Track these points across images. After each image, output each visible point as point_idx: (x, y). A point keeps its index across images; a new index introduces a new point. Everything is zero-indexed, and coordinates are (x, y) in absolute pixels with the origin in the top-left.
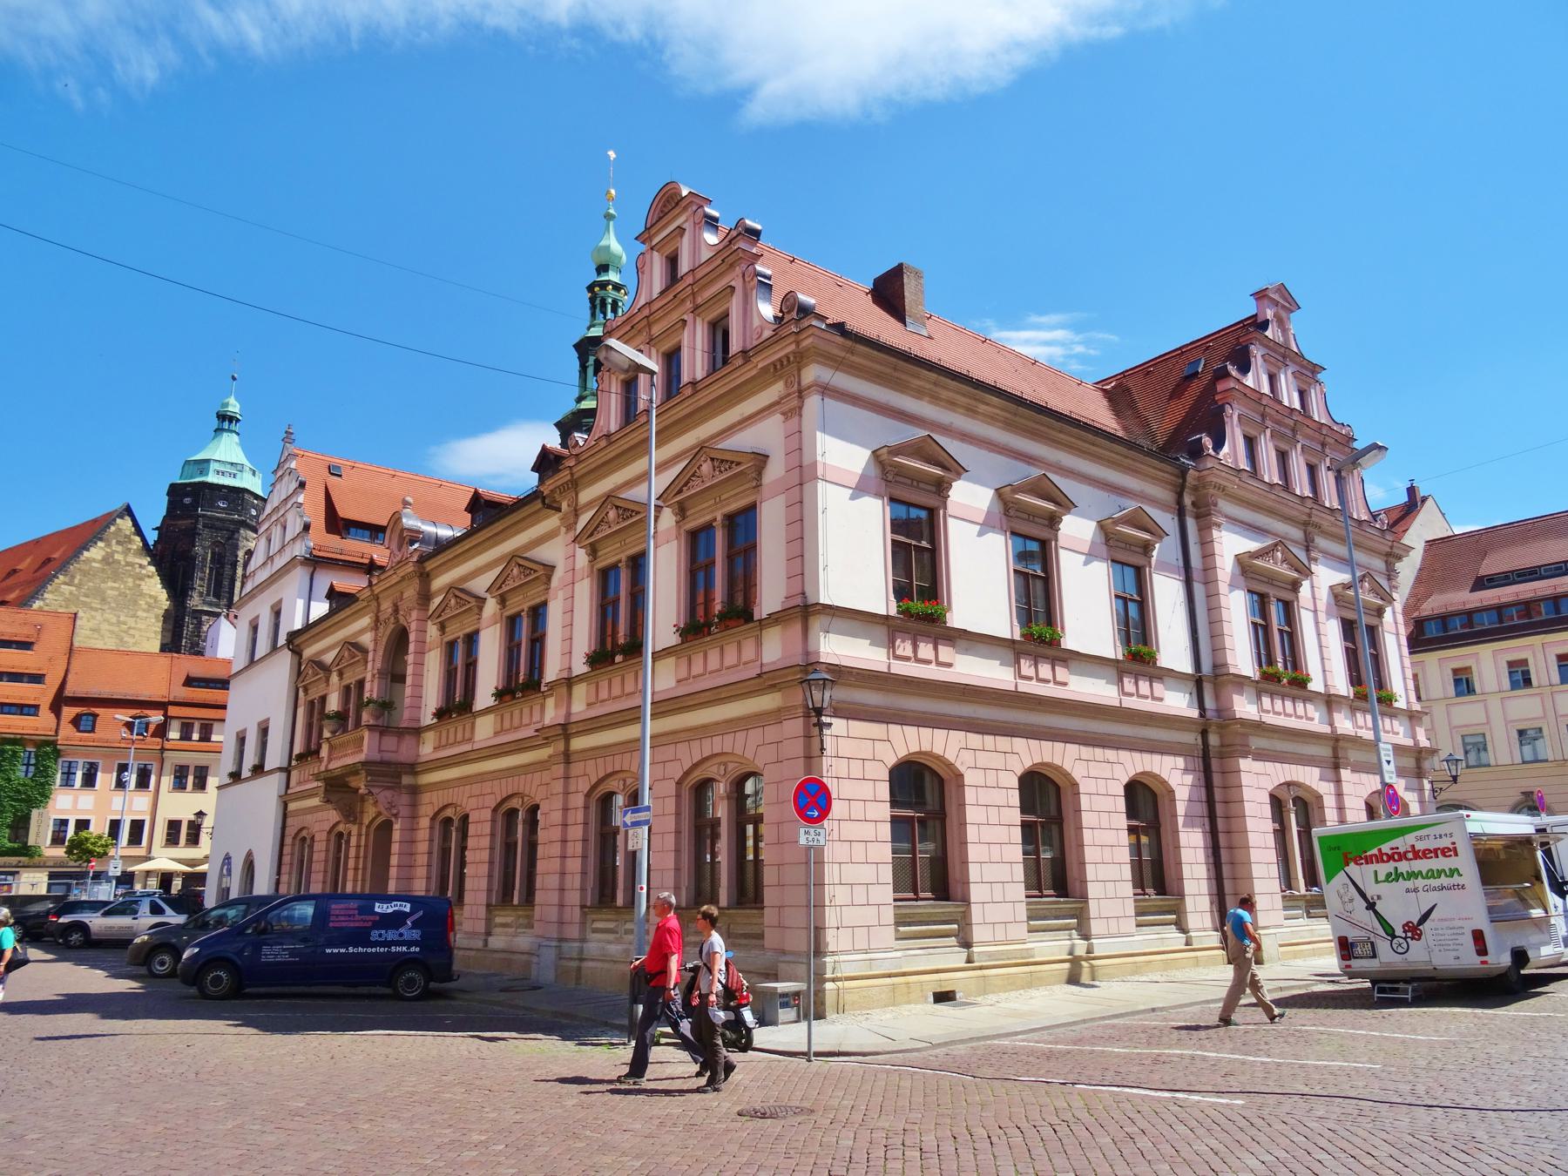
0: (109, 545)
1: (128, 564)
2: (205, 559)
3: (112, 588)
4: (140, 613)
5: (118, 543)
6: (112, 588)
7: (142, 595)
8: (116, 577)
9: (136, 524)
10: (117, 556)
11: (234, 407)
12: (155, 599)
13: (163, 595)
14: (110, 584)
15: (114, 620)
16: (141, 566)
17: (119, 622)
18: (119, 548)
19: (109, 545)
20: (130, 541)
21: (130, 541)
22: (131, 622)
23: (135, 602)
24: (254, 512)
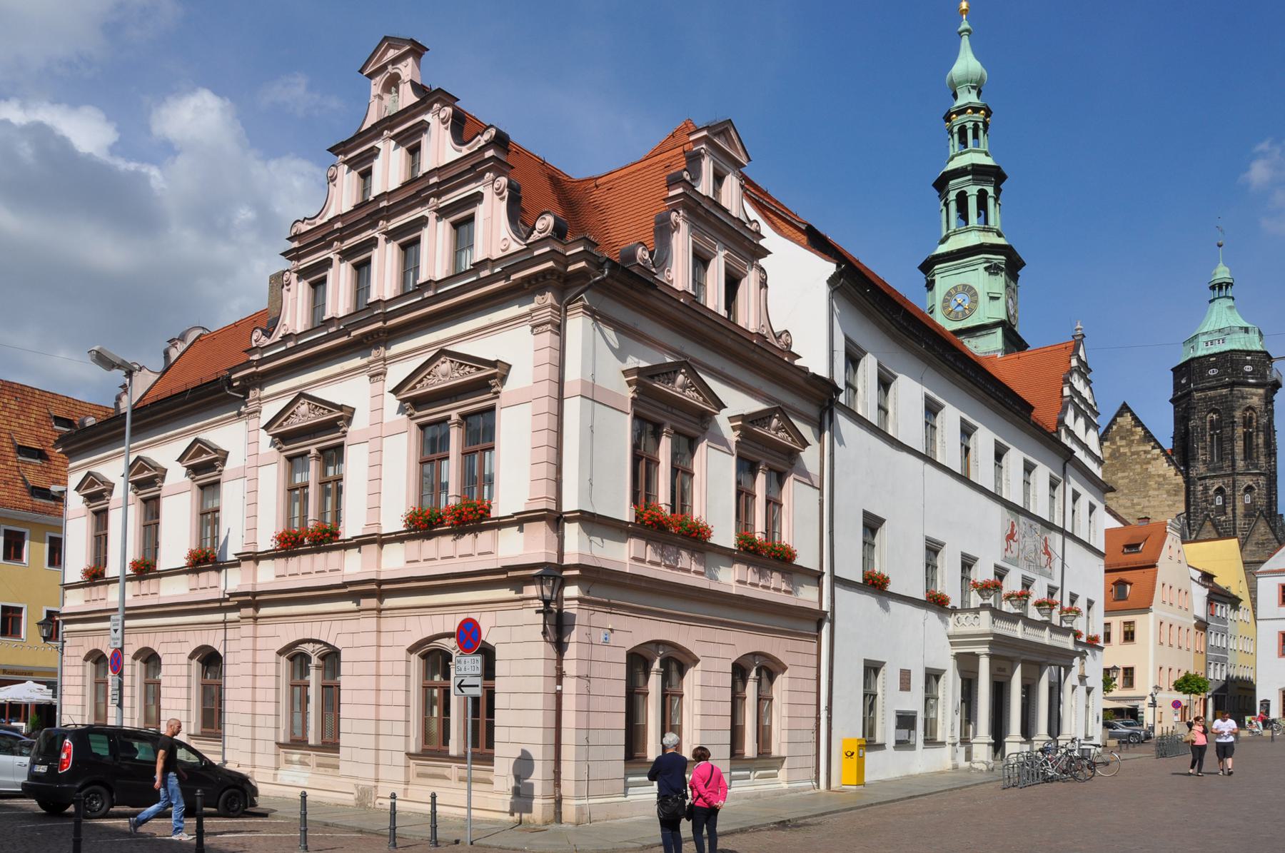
0: (1113, 442)
1: (1133, 454)
2: (1204, 429)
3: (1123, 478)
4: (1151, 493)
5: (1122, 438)
6: (1123, 478)
7: (1150, 476)
8: (1124, 467)
9: (1135, 418)
10: (1122, 450)
11: (1222, 273)
12: (1164, 477)
13: (1172, 470)
14: (1120, 475)
15: (1129, 504)
16: (1146, 452)
17: (1133, 505)
18: (1124, 443)
19: (1113, 442)
20: (1133, 433)
21: (1133, 433)
22: (1145, 502)
23: (1146, 485)
24: (1248, 368)
